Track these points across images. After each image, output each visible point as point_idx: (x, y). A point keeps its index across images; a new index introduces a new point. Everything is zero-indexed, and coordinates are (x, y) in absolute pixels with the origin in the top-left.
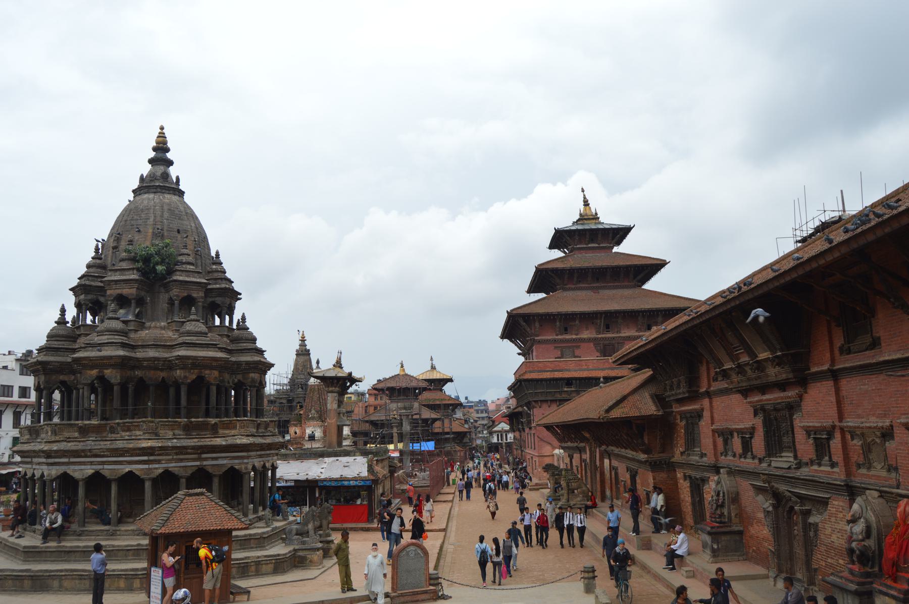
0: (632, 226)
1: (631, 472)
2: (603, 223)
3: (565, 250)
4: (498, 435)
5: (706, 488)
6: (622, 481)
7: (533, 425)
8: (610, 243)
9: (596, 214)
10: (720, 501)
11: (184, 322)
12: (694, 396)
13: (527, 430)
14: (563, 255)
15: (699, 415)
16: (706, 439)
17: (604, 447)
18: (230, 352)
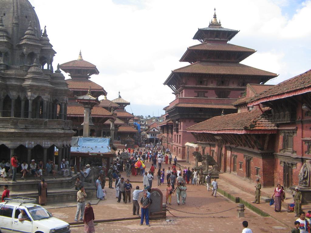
0: (238, 31)
1: (247, 158)
2: (223, 28)
3: (202, 40)
4: (151, 134)
5: (294, 168)
6: (240, 162)
7: (179, 131)
8: (226, 39)
9: (220, 23)
10: (306, 176)
11: (31, 67)
12: (293, 123)
13: (175, 133)
14: (200, 43)
15: (294, 131)
16: (297, 145)
17: (228, 145)
18: (52, 83)
